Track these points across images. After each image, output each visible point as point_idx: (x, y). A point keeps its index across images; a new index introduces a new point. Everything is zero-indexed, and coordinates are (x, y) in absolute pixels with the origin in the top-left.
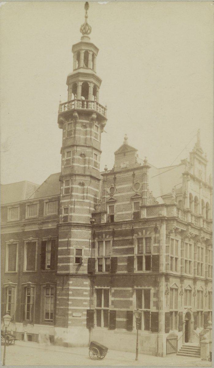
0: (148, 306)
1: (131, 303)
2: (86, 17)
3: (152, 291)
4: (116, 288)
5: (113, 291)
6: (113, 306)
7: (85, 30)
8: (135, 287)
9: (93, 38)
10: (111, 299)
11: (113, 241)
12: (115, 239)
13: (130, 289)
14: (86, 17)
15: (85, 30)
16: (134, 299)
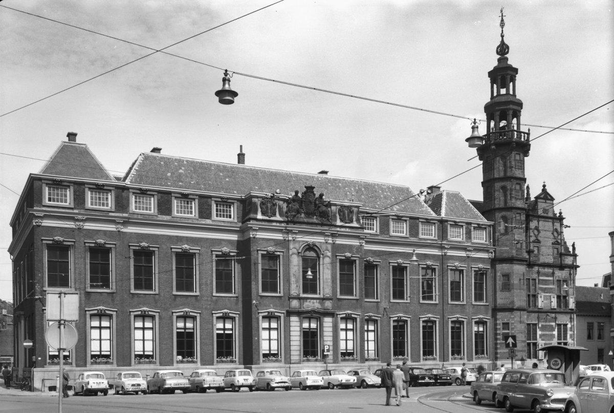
0: (565, 338)
1: (553, 336)
2: (502, 36)
3: (569, 326)
4: (543, 323)
5: (540, 326)
6: (540, 339)
7: (503, 49)
8: (557, 322)
9: (513, 60)
10: (539, 332)
11: (539, 280)
12: (541, 278)
13: (553, 324)
14: (502, 36)
15: (503, 49)
16: (555, 333)
